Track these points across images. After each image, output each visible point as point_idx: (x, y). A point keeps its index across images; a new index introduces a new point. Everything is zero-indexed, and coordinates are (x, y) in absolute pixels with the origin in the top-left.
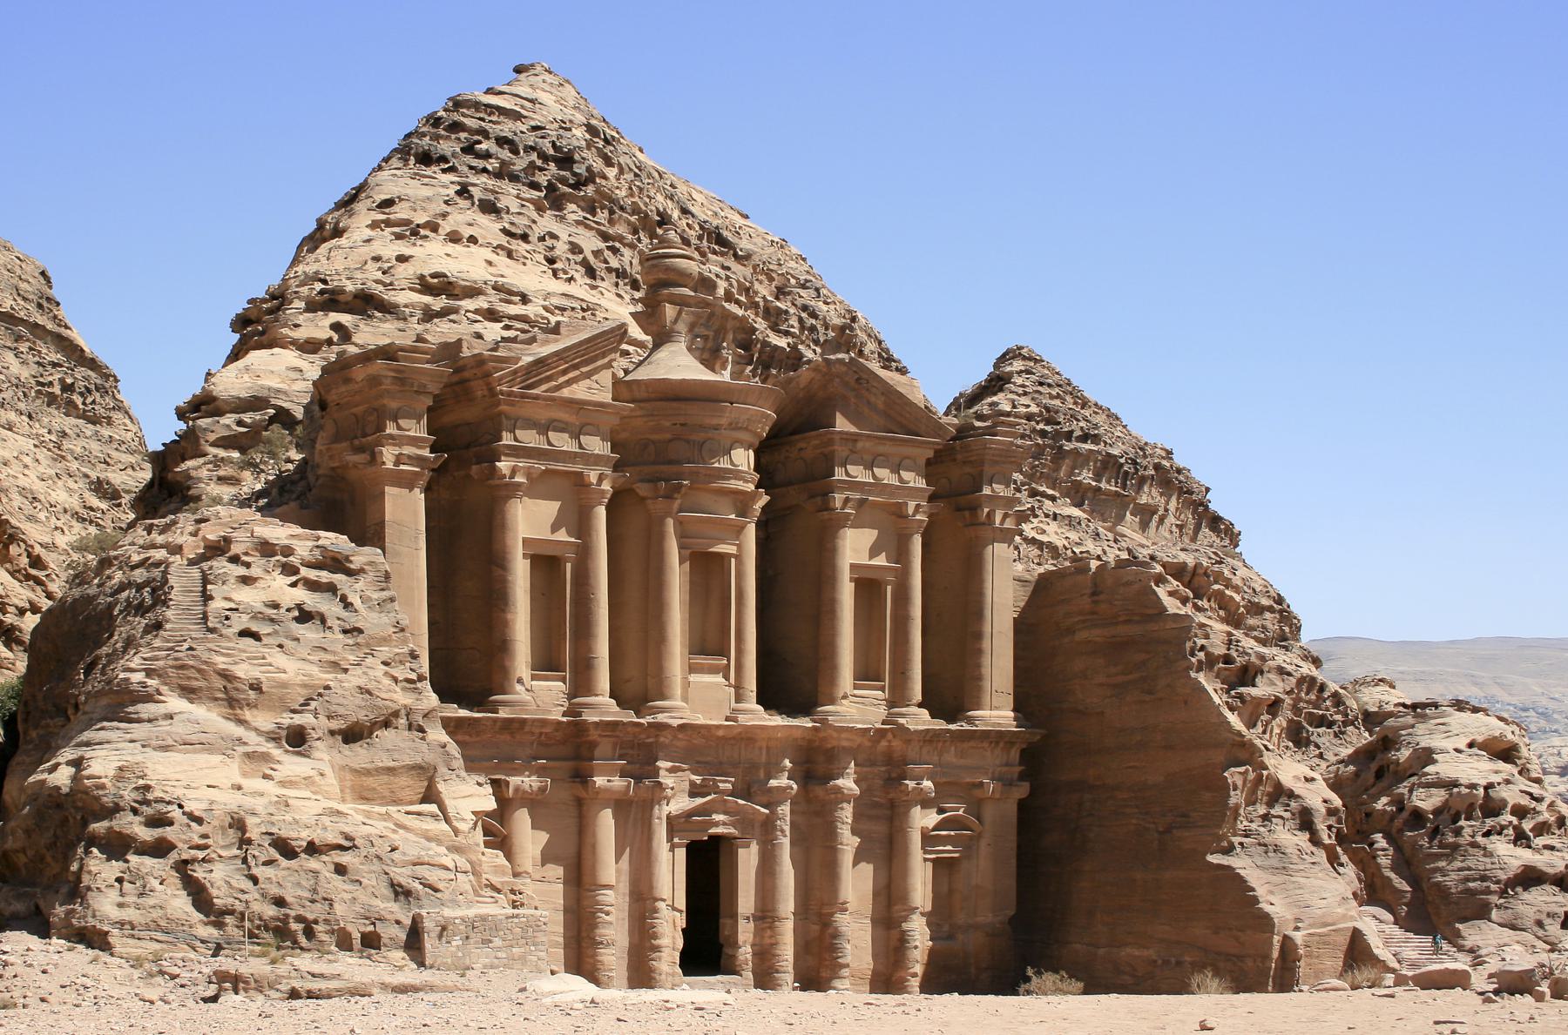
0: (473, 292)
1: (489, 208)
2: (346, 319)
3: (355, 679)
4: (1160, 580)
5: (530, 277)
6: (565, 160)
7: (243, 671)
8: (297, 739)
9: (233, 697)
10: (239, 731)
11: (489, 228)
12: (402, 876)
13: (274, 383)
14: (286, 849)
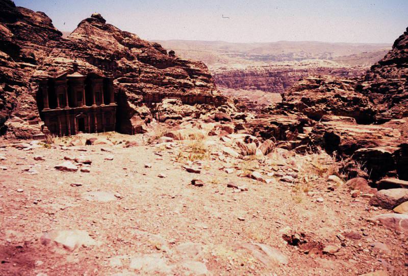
0: (60, 63)
1: (64, 52)
2: (47, 67)
3: (32, 114)
4: (126, 91)
5: (68, 61)
6: (74, 45)
7: (21, 114)
8: (26, 120)
9: (21, 116)
10: (21, 119)
11: (64, 54)
12: (33, 132)
13: (39, 75)
14: (22, 130)
